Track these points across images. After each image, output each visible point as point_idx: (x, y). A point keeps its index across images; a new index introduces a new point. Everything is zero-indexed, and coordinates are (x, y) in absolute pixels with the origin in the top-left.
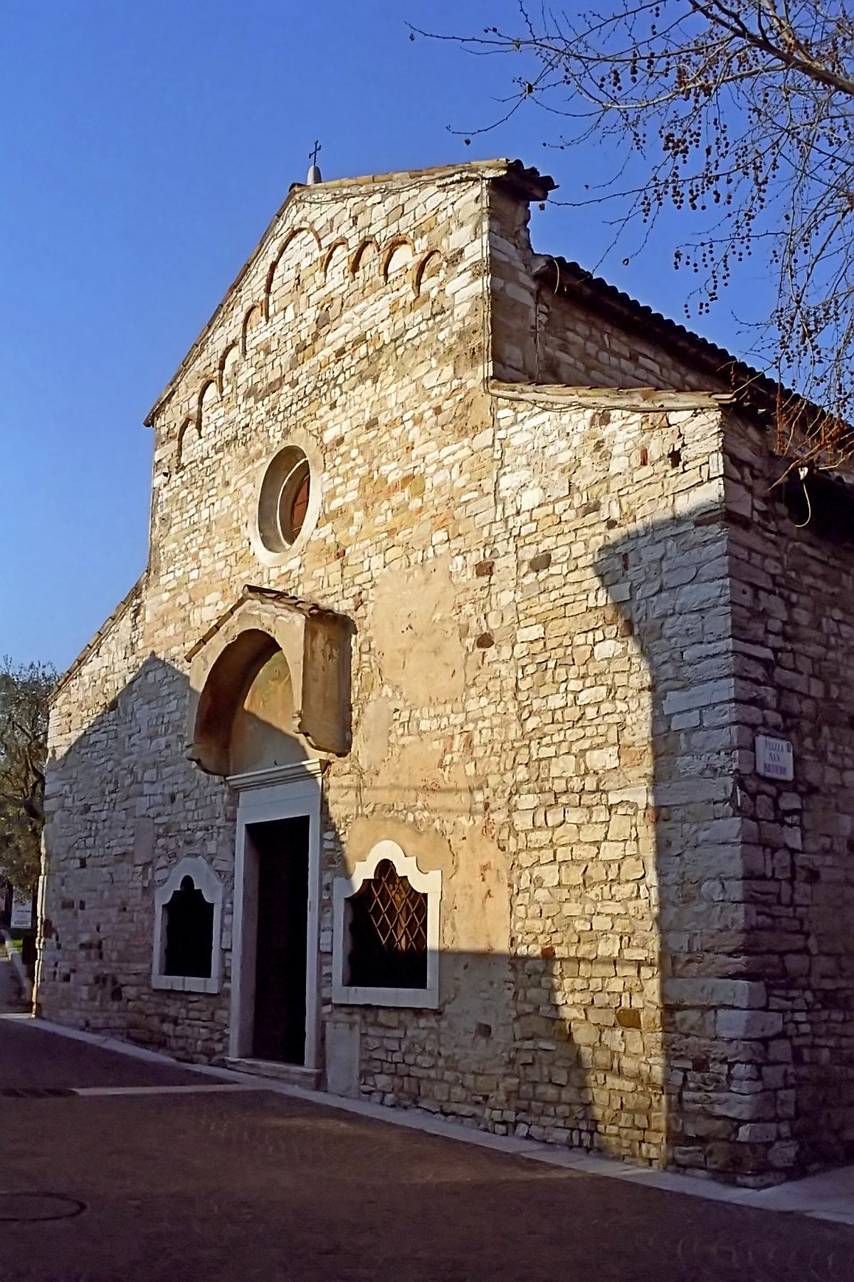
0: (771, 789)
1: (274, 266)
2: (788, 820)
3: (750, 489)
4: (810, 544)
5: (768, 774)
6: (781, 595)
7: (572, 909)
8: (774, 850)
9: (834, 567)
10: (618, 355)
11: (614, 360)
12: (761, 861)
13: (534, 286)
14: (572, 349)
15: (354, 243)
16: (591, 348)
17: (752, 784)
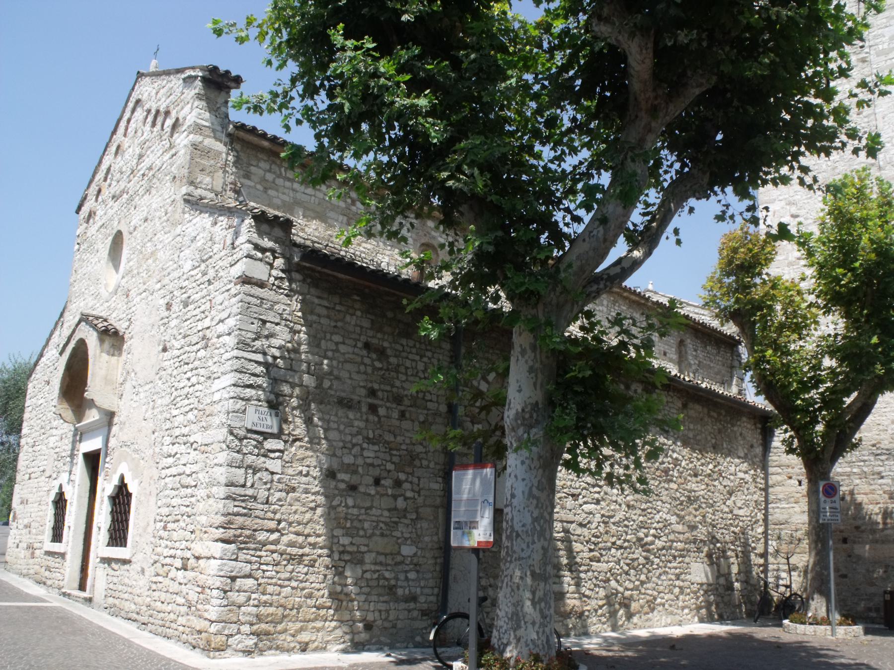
0: (261, 438)
1: (129, 121)
2: (272, 455)
3: (271, 266)
4: (319, 297)
5: (254, 428)
6: (286, 325)
7: (175, 502)
8: (256, 471)
9: (339, 311)
10: (289, 180)
11: (288, 184)
12: (239, 475)
13: (227, 140)
14: (253, 177)
15: (153, 112)
16: (270, 177)
17: (242, 433)
